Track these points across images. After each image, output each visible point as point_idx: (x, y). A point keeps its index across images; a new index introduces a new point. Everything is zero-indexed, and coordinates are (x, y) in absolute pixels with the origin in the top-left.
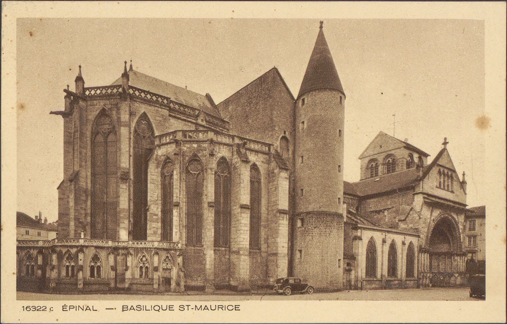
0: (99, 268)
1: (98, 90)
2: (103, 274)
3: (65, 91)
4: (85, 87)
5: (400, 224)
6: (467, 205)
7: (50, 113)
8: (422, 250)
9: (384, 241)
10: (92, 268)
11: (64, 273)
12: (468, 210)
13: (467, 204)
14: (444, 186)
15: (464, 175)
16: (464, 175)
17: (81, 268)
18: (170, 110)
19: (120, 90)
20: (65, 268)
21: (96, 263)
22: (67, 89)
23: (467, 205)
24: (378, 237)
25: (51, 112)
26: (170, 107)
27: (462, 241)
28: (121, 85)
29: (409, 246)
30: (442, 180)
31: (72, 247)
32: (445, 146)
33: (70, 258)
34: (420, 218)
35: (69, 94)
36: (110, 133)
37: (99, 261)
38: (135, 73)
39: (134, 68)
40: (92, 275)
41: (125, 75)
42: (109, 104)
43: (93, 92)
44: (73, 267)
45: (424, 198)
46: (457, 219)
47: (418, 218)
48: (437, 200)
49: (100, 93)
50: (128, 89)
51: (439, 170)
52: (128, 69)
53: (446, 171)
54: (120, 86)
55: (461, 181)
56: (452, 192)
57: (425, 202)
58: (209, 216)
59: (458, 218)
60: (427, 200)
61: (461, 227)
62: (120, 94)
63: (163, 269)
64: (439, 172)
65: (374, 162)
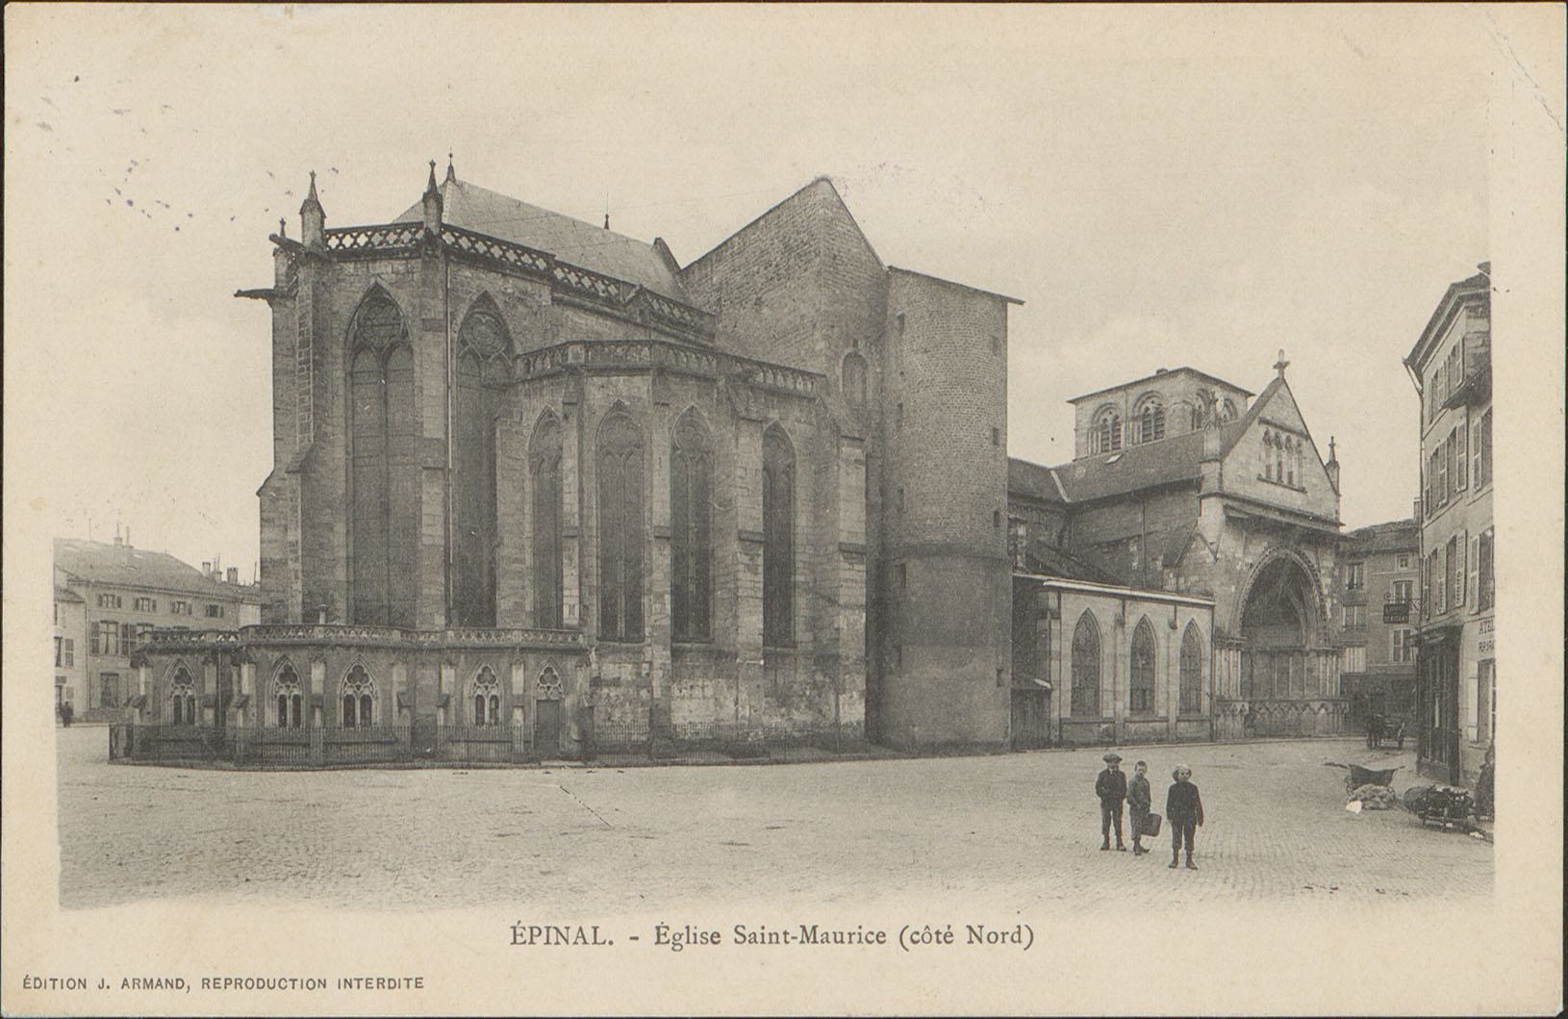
0: (366, 701)
1: (363, 236)
2: (377, 715)
3: (273, 238)
4: (327, 226)
5: (1166, 577)
6: (1342, 525)
7: (236, 296)
8: (1220, 639)
9: (1120, 623)
10: (349, 701)
11: (271, 717)
12: (1344, 538)
13: (1341, 520)
14: (1280, 478)
15: (1332, 446)
16: (1332, 446)
17: (317, 703)
18: (556, 285)
19: (420, 235)
20: (276, 703)
21: (358, 687)
22: (279, 235)
23: (1342, 525)
24: (1105, 611)
25: (239, 291)
26: (552, 279)
27: (1329, 613)
28: (422, 223)
29: (1187, 631)
30: (1273, 460)
31: (296, 646)
32: (1282, 373)
33: (288, 676)
34: (1216, 559)
35: (284, 245)
36: (393, 347)
37: (368, 684)
38: (460, 186)
39: (458, 176)
40: (349, 721)
41: (433, 196)
42: (393, 272)
43: (348, 241)
44: (297, 699)
45: (1226, 507)
48: (1258, 512)
49: (367, 244)
50: (441, 233)
51: (1267, 433)
52: (439, 182)
53: (1284, 436)
54: (419, 225)
55: (1325, 464)
56: (1302, 490)
57: (1230, 520)
58: (660, 562)
59: (1317, 558)
60: (1233, 514)
61: (1326, 581)
62: (419, 244)
63: (538, 701)
64: (1267, 440)
65: (1111, 413)
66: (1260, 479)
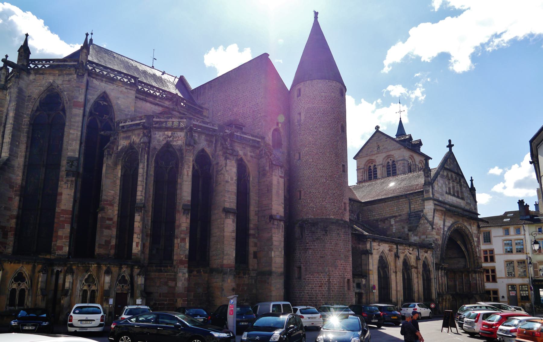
14: (454, 192)
15: (472, 180)
16: (472, 180)
34: (433, 228)
45: (435, 204)
46: (470, 230)
47: (430, 228)
56: (463, 199)
66: (446, 193)
